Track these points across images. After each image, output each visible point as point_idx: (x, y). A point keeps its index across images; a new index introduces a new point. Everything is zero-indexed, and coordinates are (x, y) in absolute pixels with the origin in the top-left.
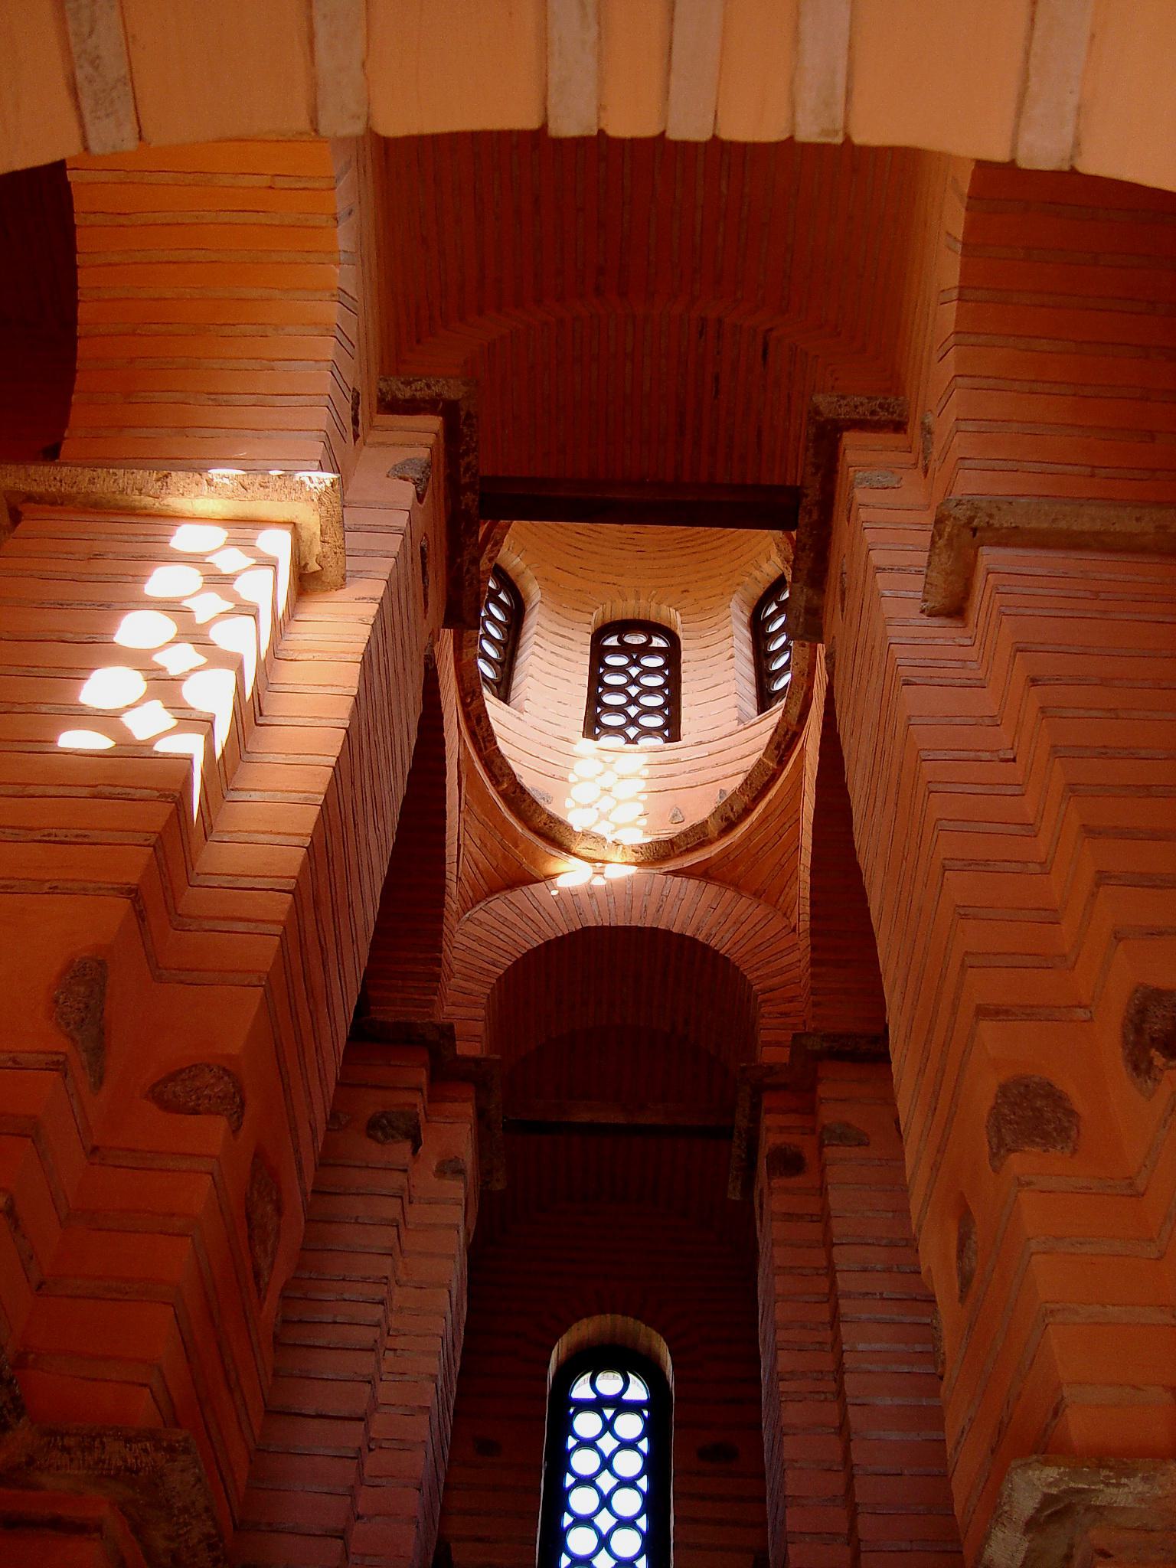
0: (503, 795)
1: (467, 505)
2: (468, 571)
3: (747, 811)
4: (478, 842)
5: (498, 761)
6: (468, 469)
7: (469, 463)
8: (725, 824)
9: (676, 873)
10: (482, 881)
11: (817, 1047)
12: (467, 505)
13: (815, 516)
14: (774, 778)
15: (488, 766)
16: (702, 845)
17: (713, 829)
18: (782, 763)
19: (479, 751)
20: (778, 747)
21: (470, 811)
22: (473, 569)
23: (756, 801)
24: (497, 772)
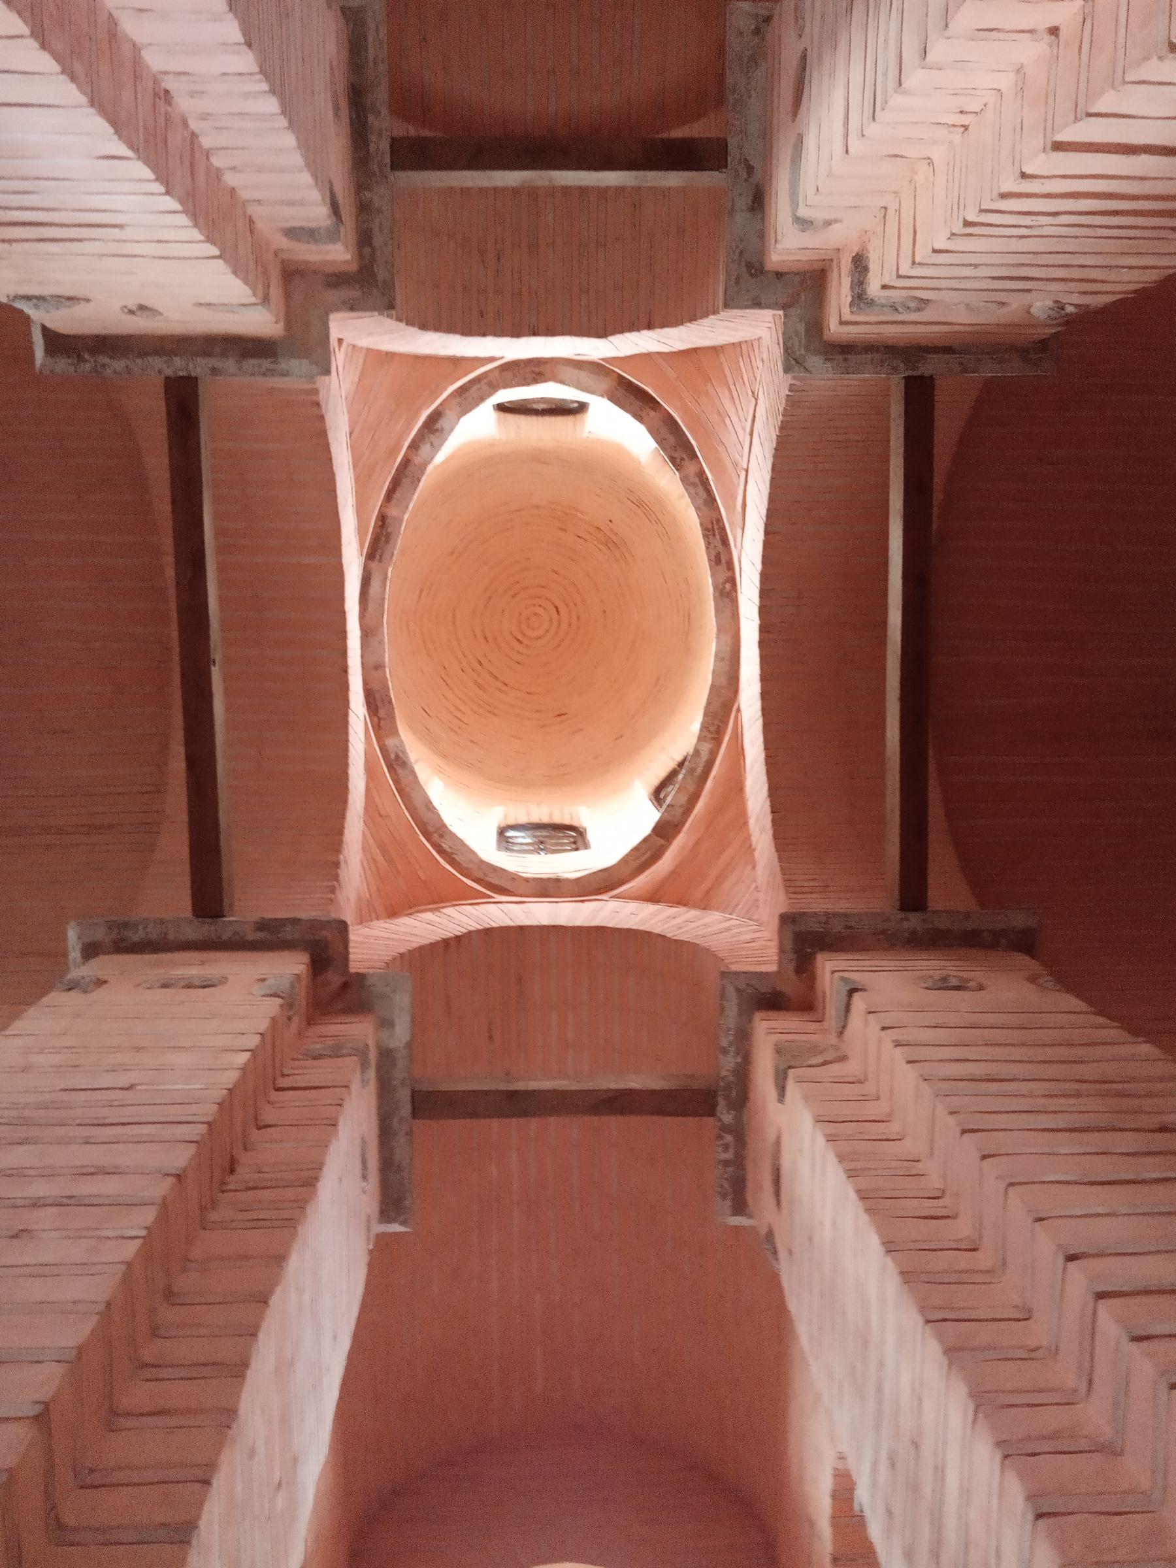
2: (731, 1043)
3: (414, 446)
5: (700, 502)
8: (438, 426)
9: (492, 359)
10: (727, 372)
13: (395, 1121)
14: (389, 496)
16: (462, 390)
17: (449, 415)
18: (382, 518)
19: (719, 520)
20: (388, 536)
21: (736, 465)
23: (406, 462)
24: (701, 490)
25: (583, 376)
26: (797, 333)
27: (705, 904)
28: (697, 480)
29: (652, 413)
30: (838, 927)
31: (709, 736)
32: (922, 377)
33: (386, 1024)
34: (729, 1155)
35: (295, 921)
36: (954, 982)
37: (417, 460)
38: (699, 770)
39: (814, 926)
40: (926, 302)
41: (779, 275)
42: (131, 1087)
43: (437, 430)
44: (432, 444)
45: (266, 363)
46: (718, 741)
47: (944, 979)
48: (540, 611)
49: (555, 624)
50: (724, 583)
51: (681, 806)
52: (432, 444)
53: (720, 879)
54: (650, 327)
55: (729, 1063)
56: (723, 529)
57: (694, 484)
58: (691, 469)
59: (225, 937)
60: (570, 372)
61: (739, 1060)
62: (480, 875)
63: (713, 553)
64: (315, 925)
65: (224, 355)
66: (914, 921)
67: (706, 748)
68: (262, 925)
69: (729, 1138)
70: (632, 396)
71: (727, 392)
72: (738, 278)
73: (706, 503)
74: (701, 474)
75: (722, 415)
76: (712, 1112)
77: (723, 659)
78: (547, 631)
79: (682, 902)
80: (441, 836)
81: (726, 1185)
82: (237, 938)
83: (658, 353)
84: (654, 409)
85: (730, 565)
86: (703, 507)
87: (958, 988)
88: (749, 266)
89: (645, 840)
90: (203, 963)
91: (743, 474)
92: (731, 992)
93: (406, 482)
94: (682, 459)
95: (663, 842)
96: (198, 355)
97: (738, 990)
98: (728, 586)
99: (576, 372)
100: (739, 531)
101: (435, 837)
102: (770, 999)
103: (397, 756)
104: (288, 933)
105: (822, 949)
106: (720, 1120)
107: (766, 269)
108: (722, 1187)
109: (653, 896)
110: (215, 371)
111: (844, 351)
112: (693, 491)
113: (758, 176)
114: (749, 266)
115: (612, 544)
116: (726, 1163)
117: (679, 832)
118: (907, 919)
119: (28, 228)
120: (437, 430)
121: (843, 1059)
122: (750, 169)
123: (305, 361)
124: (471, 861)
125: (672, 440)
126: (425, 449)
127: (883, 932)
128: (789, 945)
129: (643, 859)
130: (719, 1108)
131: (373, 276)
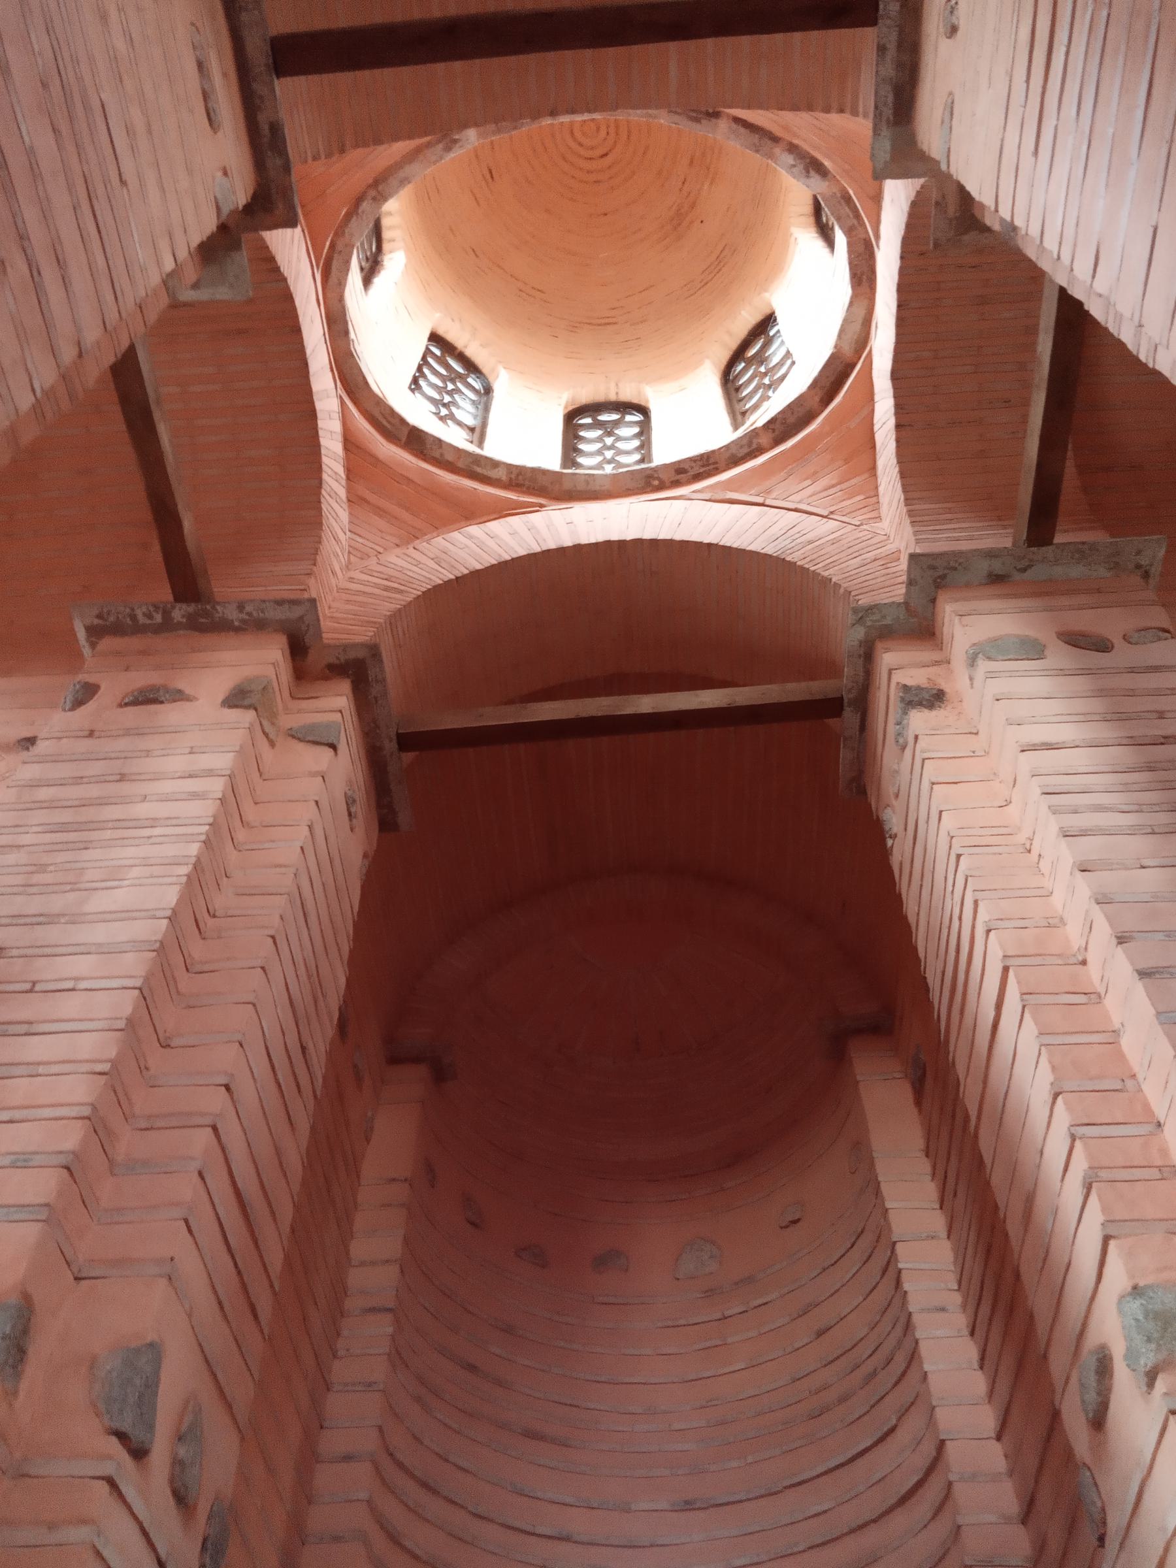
0: (778, 442)
1: (183, 616)
2: (249, 614)
4: (808, 482)
5: (734, 450)
6: (150, 617)
7: (144, 614)
8: (812, 173)
9: (877, 237)
11: (887, 145)
12: (183, 616)
15: (735, 461)
16: (848, 200)
19: (717, 471)
21: (768, 492)
22: (248, 608)
24: (746, 450)
25: (857, 327)
26: (884, 617)
27: (354, 500)
28: (754, 446)
29: (817, 399)
30: (375, 690)
31: (513, 476)
32: (842, 709)
33: (196, 286)
34: (142, 619)
35: (287, 168)
36: (353, 810)
37: (777, 151)
38: (479, 470)
39: (372, 674)
40: (903, 748)
41: (933, 601)
42: (123, 182)
43: (808, 172)
44: (794, 166)
45: (888, 112)
46: (510, 485)
47: (354, 801)
48: (603, 133)
49: (589, 154)
50: (658, 478)
51: (442, 455)
52: (794, 166)
53: (380, 512)
54: (898, 426)
55: (232, 614)
56: (709, 475)
57: (750, 443)
58: (764, 440)
59: (255, 86)
60: (861, 312)
61: (236, 624)
62: (340, 246)
63: (687, 467)
64: (286, 192)
65: (900, 65)
66: (390, 746)
67: (500, 474)
68: (276, 129)
69: (158, 618)
70: (837, 373)
71: (834, 482)
72: (933, 568)
73: (733, 456)
74: (760, 451)
75: (814, 476)
76: (179, 598)
77: (588, 483)
78: (581, 145)
79: (351, 473)
80: (374, 199)
81: (112, 619)
82: (258, 101)
83: (873, 410)
84: (821, 401)
85: (676, 484)
86: (728, 455)
87: (350, 814)
88: (943, 577)
89: (403, 421)
90: (225, 75)
91: (759, 500)
92: (297, 612)
93: (755, 138)
94: (774, 430)
95: (404, 439)
96: (900, 33)
97: (301, 618)
98: (656, 483)
99: (860, 321)
100: (707, 496)
101: (372, 193)
102: (298, 648)
103: (455, 141)
104: (273, 162)
105: (352, 682)
106: (173, 608)
107: (940, 592)
108: (109, 613)
109: (350, 442)
110: (882, 49)
111: (868, 656)
112: (745, 442)
113: (1017, 576)
114: (943, 577)
115: (679, 221)
116: (133, 617)
117: (416, 456)
118: (391, 741)
119: (1040, 90)
120: (808, 172)
121: (272, 744)
122: (1024, 570)
123: (888, 157)
124: (352, 235)
125: (791, 420)
126: (790, 159)
127: (378, 727)
128: (352, 655)
129: (385, 423)
130: (184, 606)
131: (966, 232)
